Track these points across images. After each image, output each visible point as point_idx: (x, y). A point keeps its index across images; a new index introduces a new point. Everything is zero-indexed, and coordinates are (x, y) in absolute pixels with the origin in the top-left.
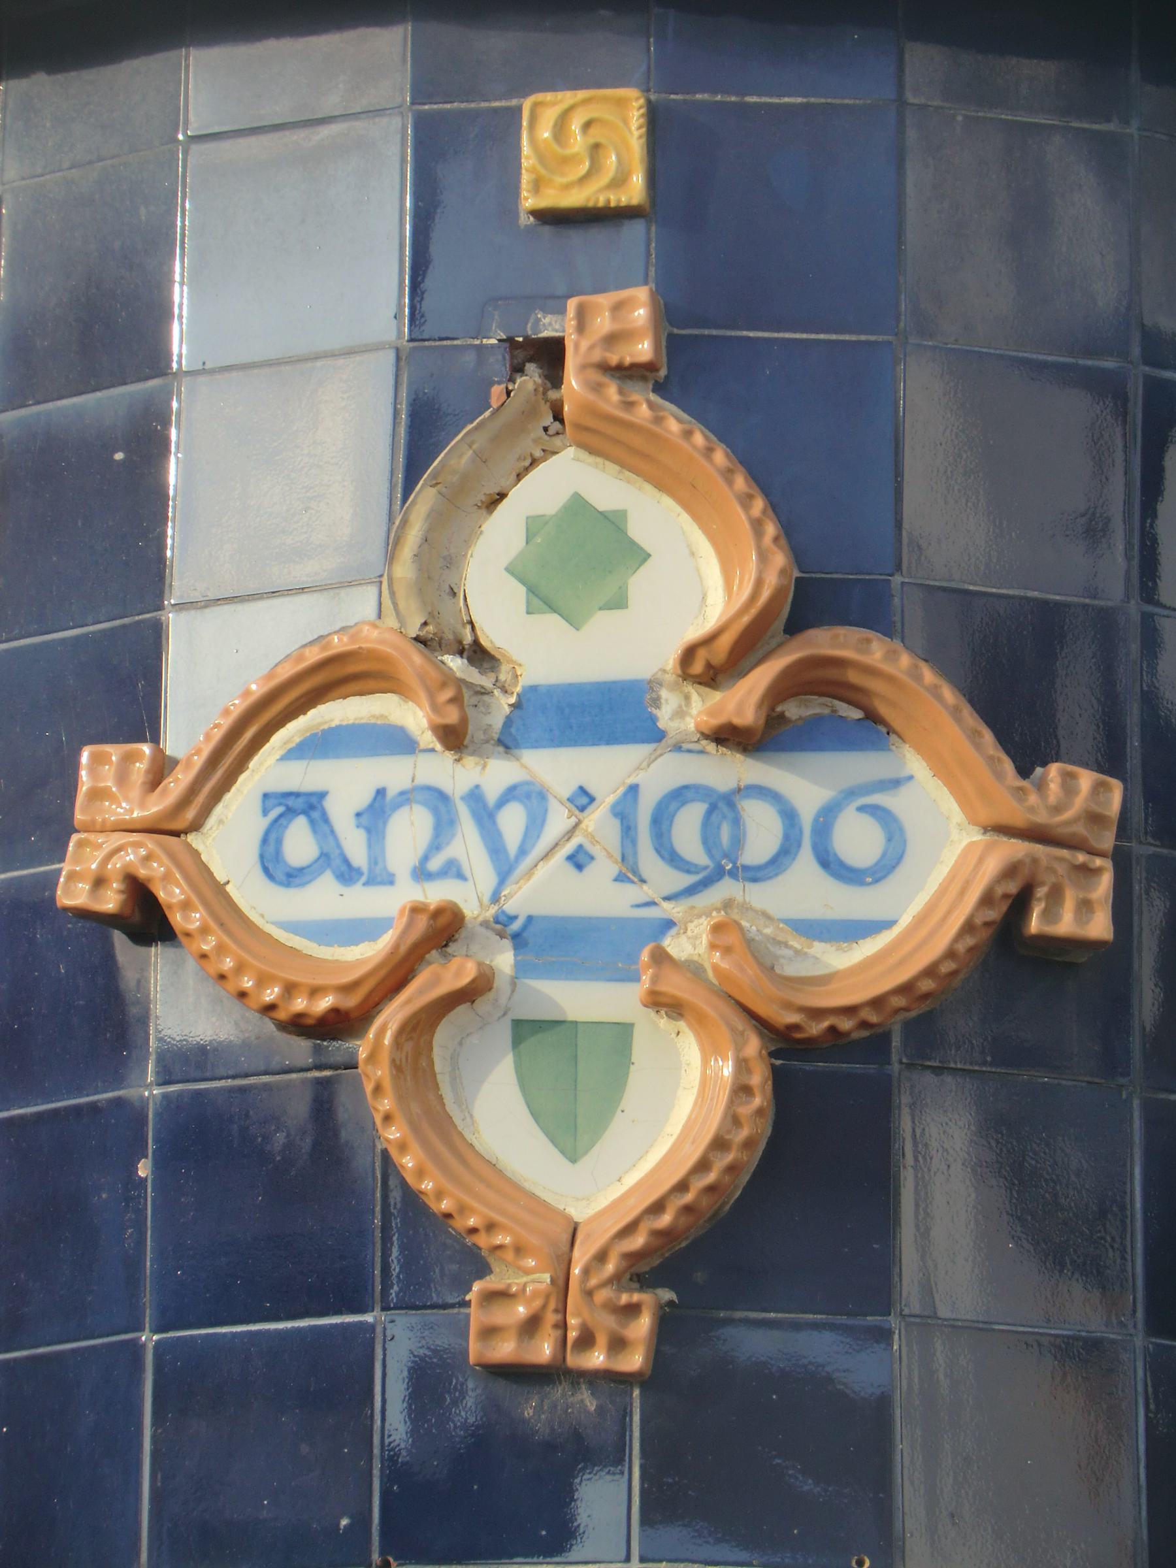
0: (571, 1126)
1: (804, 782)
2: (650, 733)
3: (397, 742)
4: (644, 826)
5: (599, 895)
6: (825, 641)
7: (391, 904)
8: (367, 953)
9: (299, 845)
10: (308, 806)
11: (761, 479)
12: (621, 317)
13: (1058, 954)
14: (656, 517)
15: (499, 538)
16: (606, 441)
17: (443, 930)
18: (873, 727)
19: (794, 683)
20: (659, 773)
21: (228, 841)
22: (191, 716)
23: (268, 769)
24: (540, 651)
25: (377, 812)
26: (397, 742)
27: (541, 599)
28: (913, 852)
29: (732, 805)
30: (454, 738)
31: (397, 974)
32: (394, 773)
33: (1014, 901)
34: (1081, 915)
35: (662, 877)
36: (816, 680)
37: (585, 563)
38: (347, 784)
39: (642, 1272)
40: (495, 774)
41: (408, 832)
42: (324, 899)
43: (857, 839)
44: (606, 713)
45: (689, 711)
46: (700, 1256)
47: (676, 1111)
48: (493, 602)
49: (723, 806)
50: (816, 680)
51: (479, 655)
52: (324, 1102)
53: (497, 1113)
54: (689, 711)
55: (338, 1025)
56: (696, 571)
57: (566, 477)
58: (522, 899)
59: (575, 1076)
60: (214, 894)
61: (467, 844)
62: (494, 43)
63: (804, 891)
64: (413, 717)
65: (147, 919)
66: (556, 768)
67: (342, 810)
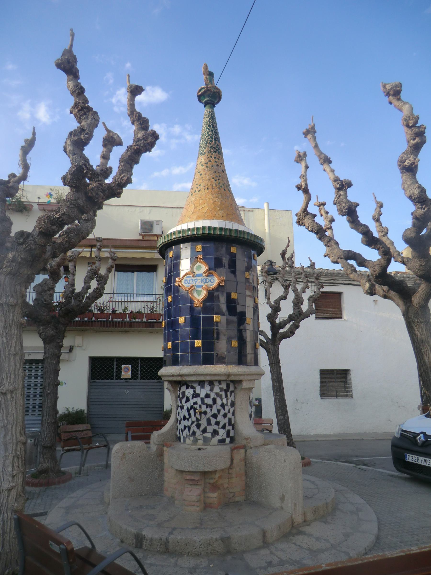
0: (199, 295)
1: (210, 278)
2: (202, 276)
3: (191, 277)
4: (202, 281)
5: (200, 284)
6: (210, 271)
7: (190, 285)
8: (189, 287)
9: (186, 282)
10: (187, 280)
11: (207, 264)
12: (201, 256)
13: (222, 286)
14: (202, 266)
15: (195, 267)
16: (200, 262)
17: (193, 286)
18: (213, 275)
19: (209, 273)
20: (203, 278)
21: (183, 282)
22: (181, 276)
23: (185, 278)
24: (197, 272)
25: (190, 280)
26: (191, 277)
27: (197, 270)
28: (214, 282)
29: (105, 446)
30: (193, 277)
31: (190, 288)
32: (190, 278)
33: (219, 283)
34: (223, 284)
35: (203, 283)
36: (210, 273)
37: (199, 268)
38: (188, 279)
39: (202, 302)
40: (195, 278)
41: (191, 281)
42: (187, 285)
43: (212, 281)
44: (200, 275)
45: (204, 275)
46: (205, 301)
47: (204, 294)
48: (195, 270)
49: (206, 279)
50: (210, 273)
51: (194, 273)
52: (187, 294)
53: (195, 294)
54: (204, 275)
55: (188, 291)
56: (204, 268)
57: (198, 264)
58: (196, 284)
59: (199, 293)
60: (182, 284)
61: (194, 282)
62: (195, 243)
63: (210, 283)
64: (191, 276)
65: (179, 286)
66: (198, 278)
67: (188, 280)
